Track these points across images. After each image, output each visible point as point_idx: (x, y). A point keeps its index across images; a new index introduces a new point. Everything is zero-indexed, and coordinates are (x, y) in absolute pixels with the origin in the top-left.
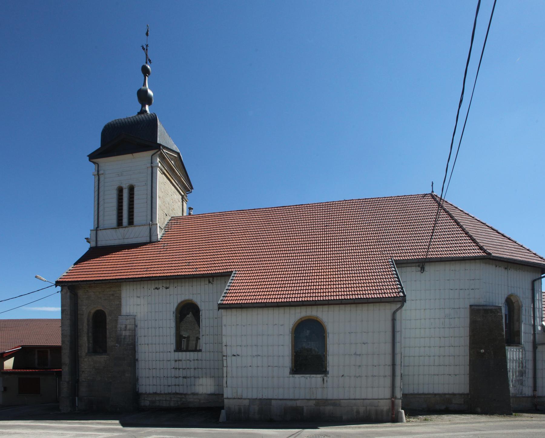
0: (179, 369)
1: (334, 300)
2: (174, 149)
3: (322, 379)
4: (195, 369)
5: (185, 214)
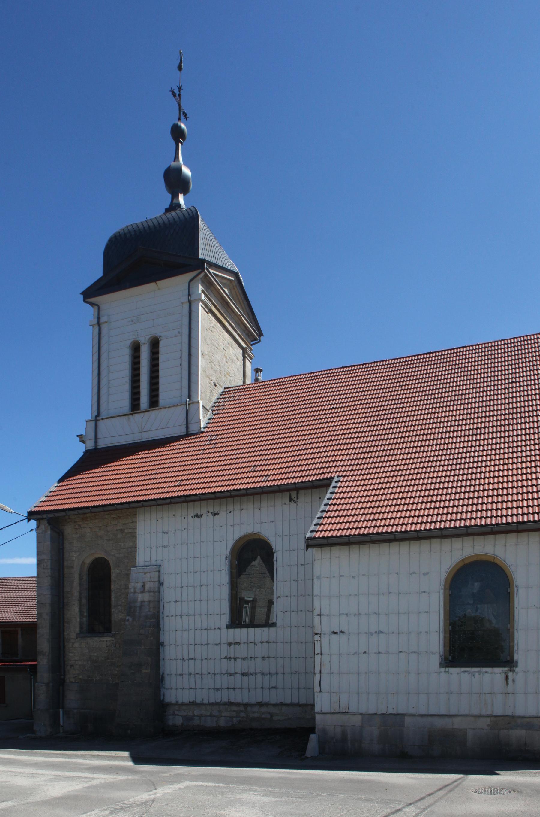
0: (235, 659)
1: (529, 521)
2: (229, 267)
3: (503, 676)
4: (263, 658)
5: (248, 382)
